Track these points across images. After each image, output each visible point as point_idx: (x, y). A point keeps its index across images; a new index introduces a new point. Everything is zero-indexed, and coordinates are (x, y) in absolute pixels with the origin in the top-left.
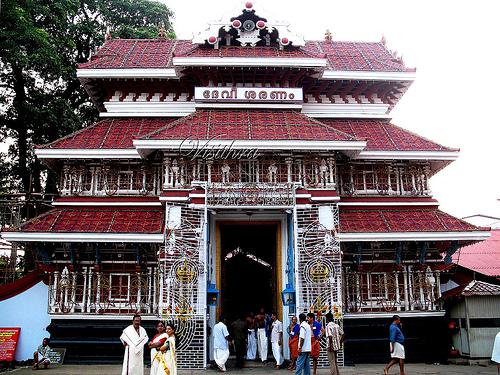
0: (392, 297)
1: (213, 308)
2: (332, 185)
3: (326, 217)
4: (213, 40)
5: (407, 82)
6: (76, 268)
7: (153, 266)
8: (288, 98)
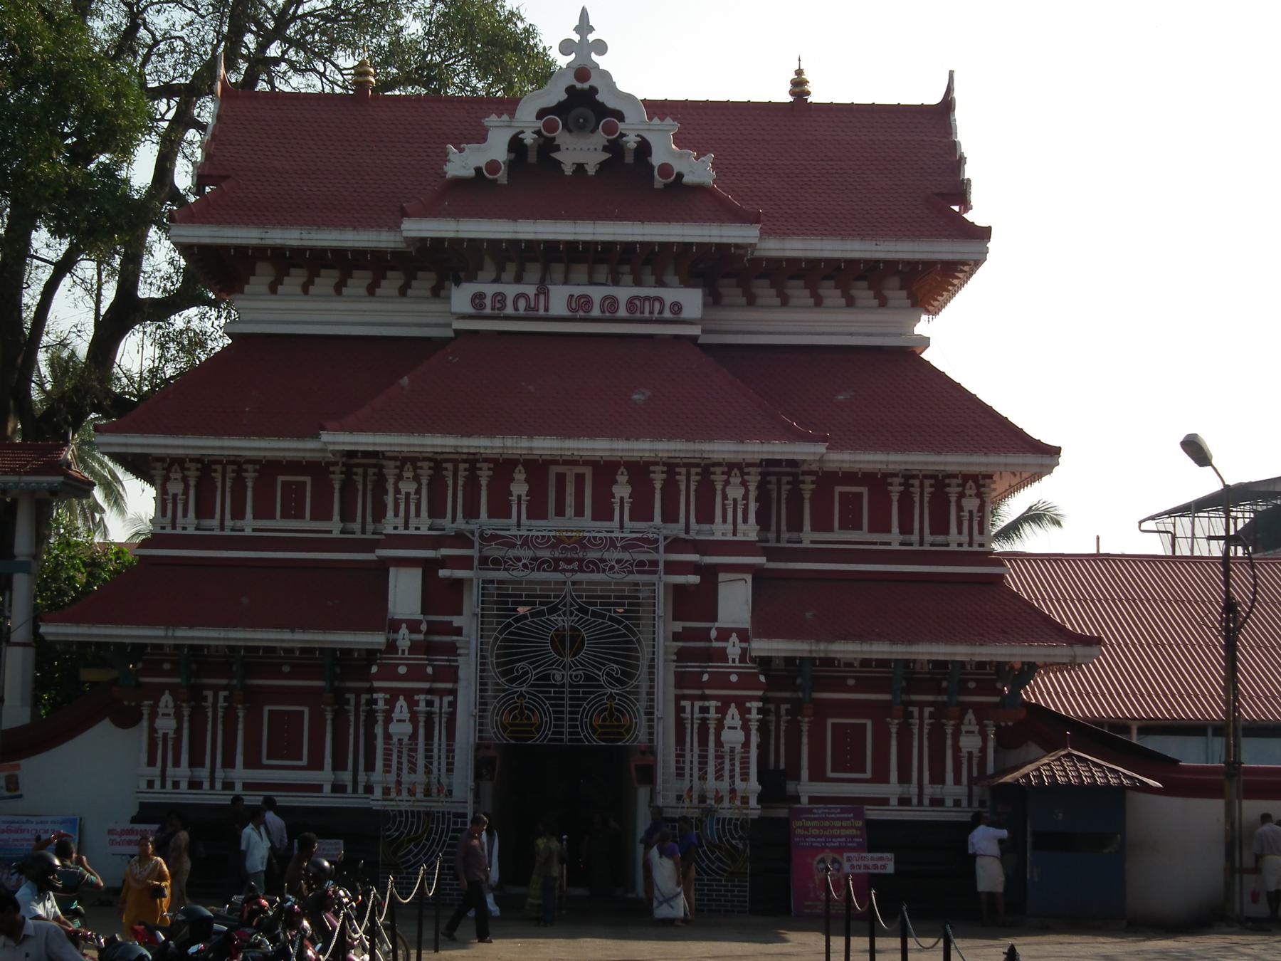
1: (487, 787)
2: (750, 532)
3: (735, 601)
4: (493, 166)
5: (965, 263)
6: (195, 694)
7: (358, 692)
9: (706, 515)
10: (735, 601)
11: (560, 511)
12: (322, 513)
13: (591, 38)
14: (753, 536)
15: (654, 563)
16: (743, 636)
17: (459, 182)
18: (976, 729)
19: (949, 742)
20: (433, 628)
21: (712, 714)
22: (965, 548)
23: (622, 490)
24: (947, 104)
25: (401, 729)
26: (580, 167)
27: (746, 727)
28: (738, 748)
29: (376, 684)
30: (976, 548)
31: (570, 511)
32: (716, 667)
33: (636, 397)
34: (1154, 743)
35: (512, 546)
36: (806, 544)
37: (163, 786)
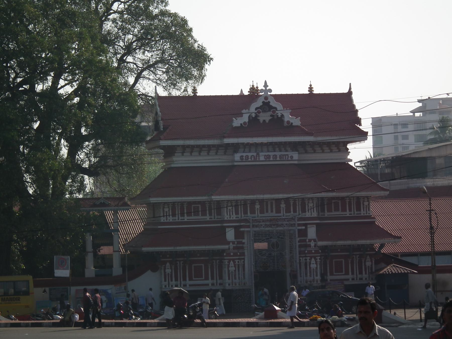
0: (347, 273)
3: (312, 232)
4: (245, 123)
8: (289, 159)
9: (304, 211)
10: (312, 232)
11: (267, 212)
12: (204, 214)
13: (268, 88)
14: (316, 216)
15: (294, 224)
16: (315, 240)
17: (236, 128)
18: (370, 260)
19: (363, 264)
20: (238, 243)
21: (308, 260)
22: (365, 215)
23: (283, 206)
24: (350, 93)
25: (232, 269)
26: (264, 121)
27: (316, 264)
28: (315, 269)
29: (225, 258)
30: (368, 215)
31: (269, 211)
32: (309, 249)
33: (285, 182)
34: (405, 259)
35: (260, 222)
36: (326, 216)
37: (169, 286)
